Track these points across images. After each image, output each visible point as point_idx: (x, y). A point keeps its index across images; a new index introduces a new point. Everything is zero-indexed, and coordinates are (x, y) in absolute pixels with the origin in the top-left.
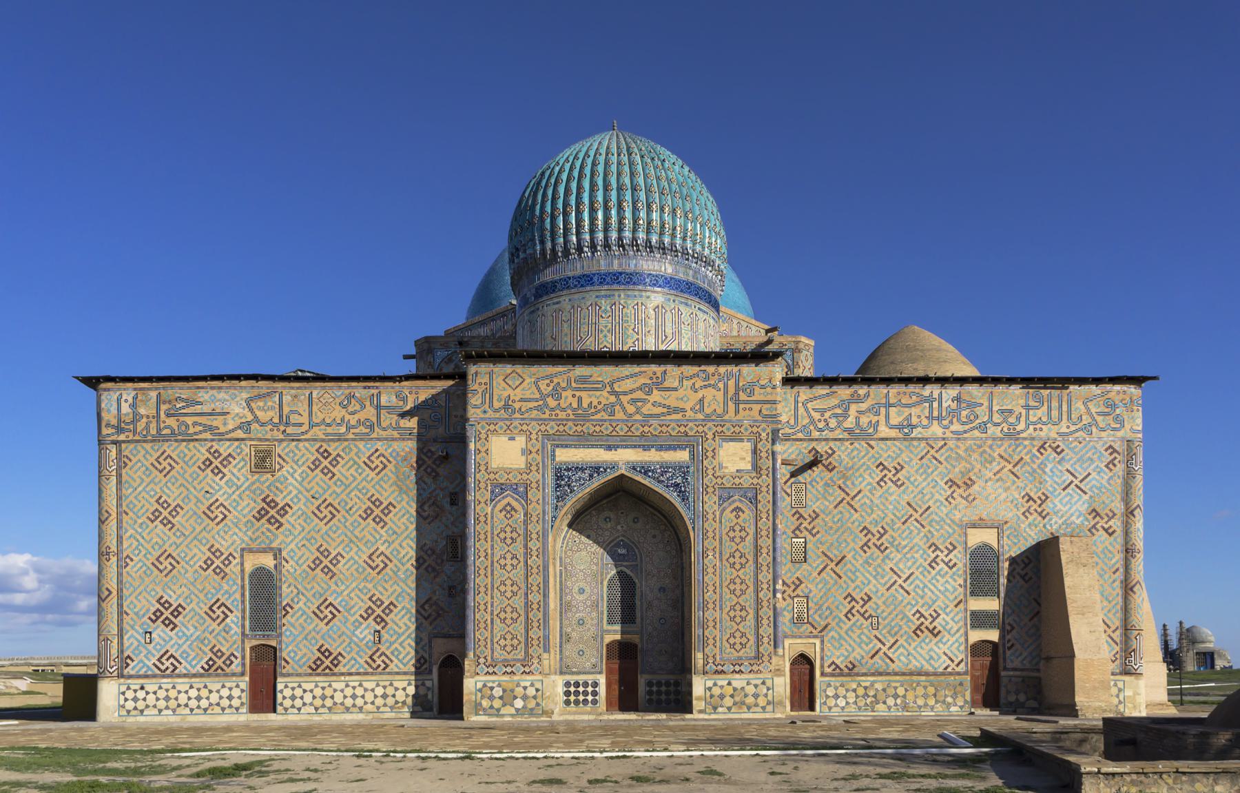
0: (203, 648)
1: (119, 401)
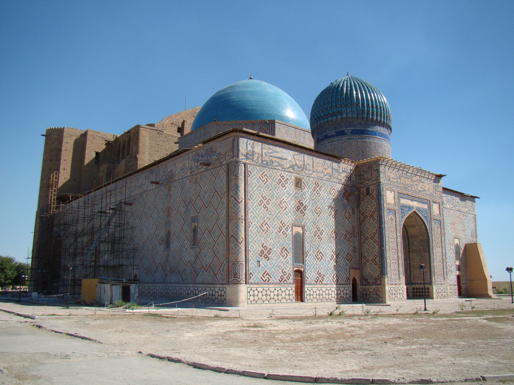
0: (279, 270)
1: (247, 143)
